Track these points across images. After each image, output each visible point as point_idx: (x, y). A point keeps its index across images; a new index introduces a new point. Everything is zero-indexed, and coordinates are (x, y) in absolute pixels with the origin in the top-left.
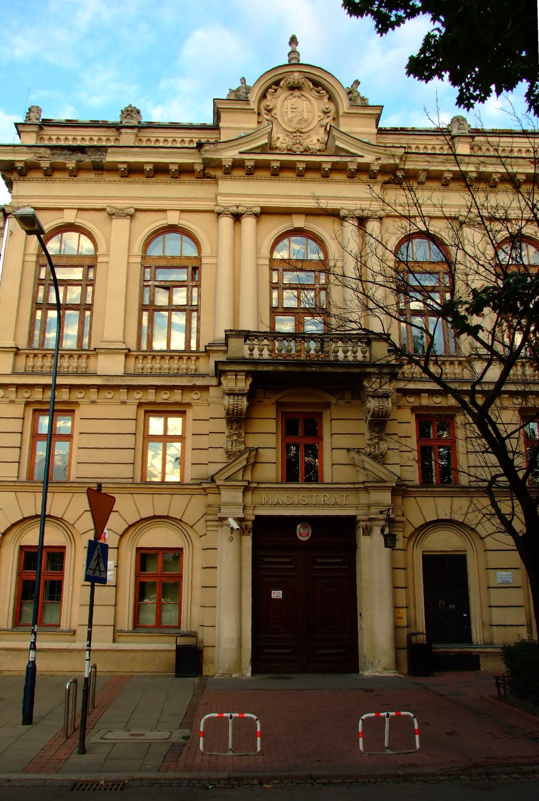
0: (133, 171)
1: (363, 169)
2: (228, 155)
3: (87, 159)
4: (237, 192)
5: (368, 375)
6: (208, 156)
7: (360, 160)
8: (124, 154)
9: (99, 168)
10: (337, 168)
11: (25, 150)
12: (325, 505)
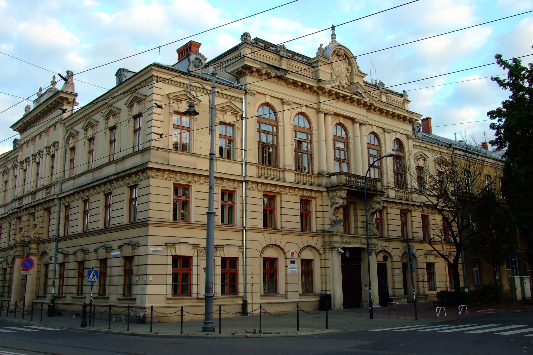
0: (295, 83)
1: (365, 103)
2: (328, 87)
3: (280, 74)
4: (331, 105)
5: (376, 195)
6: (322, 85)
7: (365, 100)
8: (293, 76)
9: (280, 78)
10: (358, 101)
11: (258, 63)
12: (359, 243)
